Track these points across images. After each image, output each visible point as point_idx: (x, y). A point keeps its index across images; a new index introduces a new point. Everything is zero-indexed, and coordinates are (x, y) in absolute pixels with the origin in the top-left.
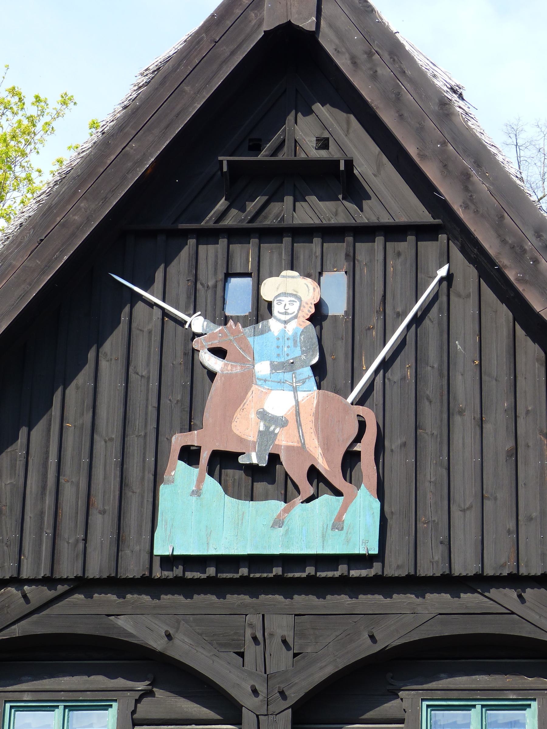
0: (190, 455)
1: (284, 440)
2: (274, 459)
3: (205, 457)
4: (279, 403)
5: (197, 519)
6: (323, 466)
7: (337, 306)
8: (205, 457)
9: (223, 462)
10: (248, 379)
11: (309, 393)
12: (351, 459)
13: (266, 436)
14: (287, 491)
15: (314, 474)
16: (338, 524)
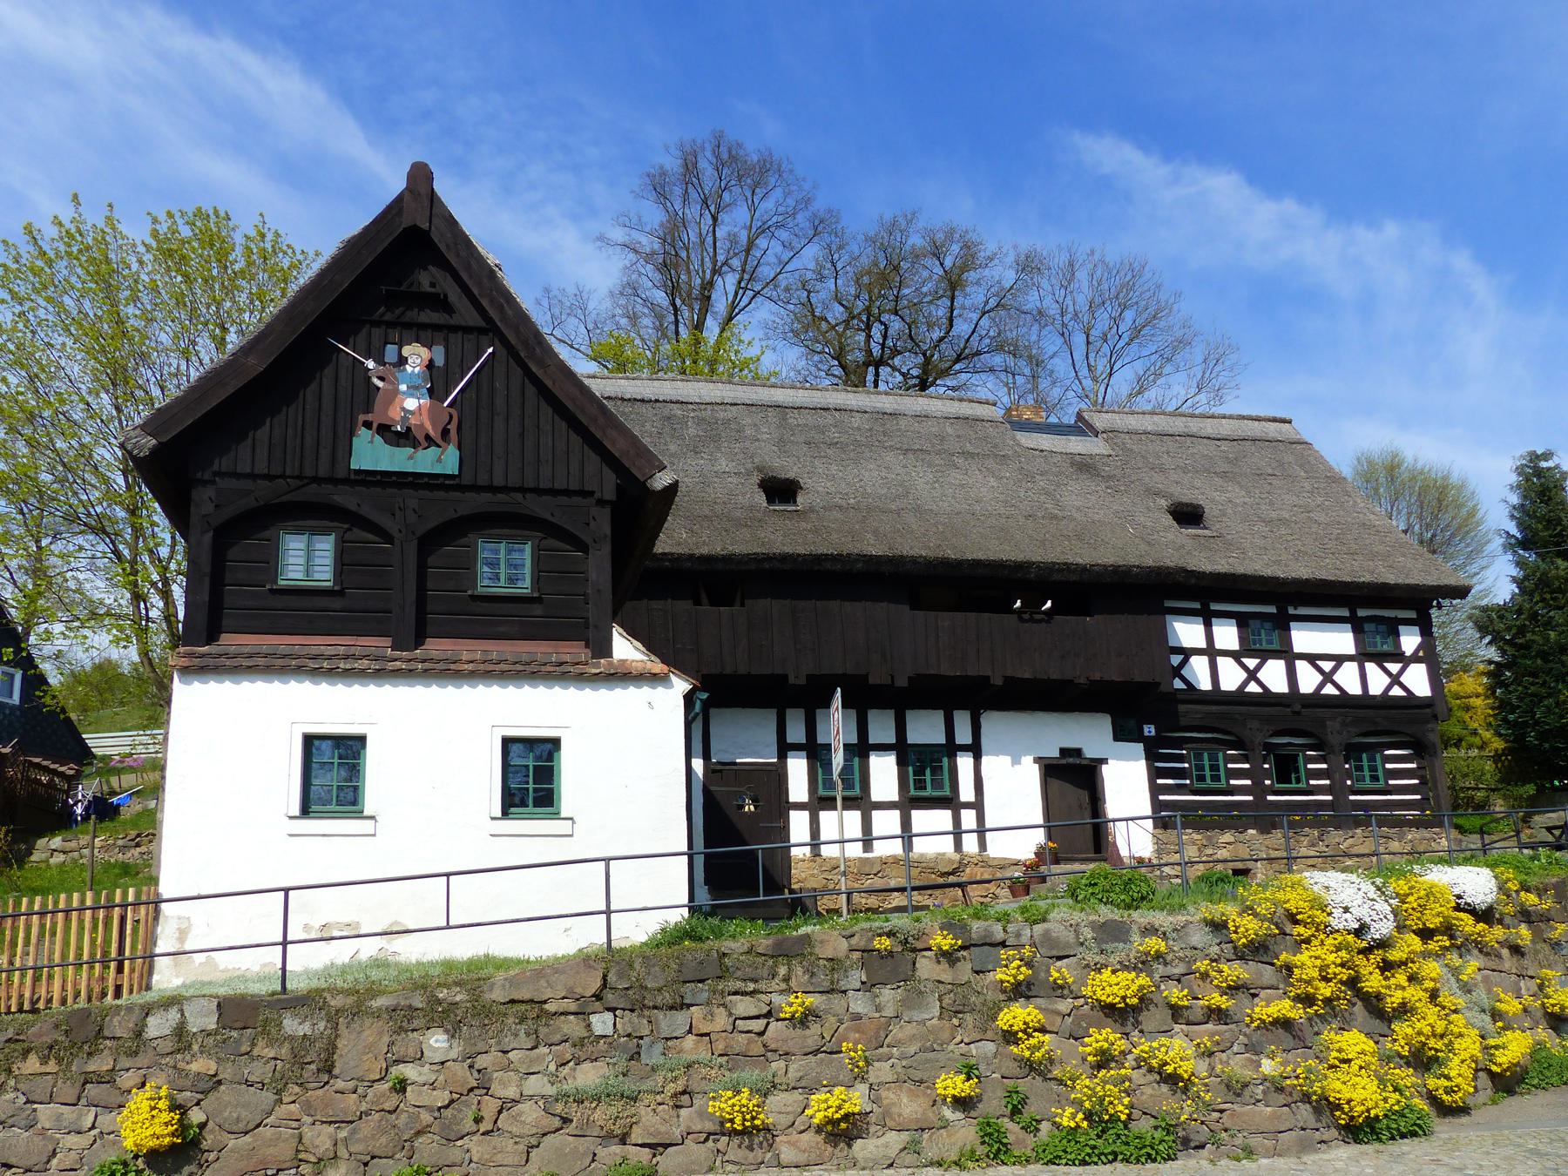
0: (368, 425)
1: (413, 421)
2: (409, 429)
3: (375, 426)
4: (411, 404)
5: (370, 453)
6: (432, 433)
7: (440, 361)
8: (375, 426)
9: (384, 430)
10: (396, 392)
11: (425, 401)
12: (445, 433)
13: (405, 419)
14: (415, 444)
15: (428, 437)
16: (439, 460)
